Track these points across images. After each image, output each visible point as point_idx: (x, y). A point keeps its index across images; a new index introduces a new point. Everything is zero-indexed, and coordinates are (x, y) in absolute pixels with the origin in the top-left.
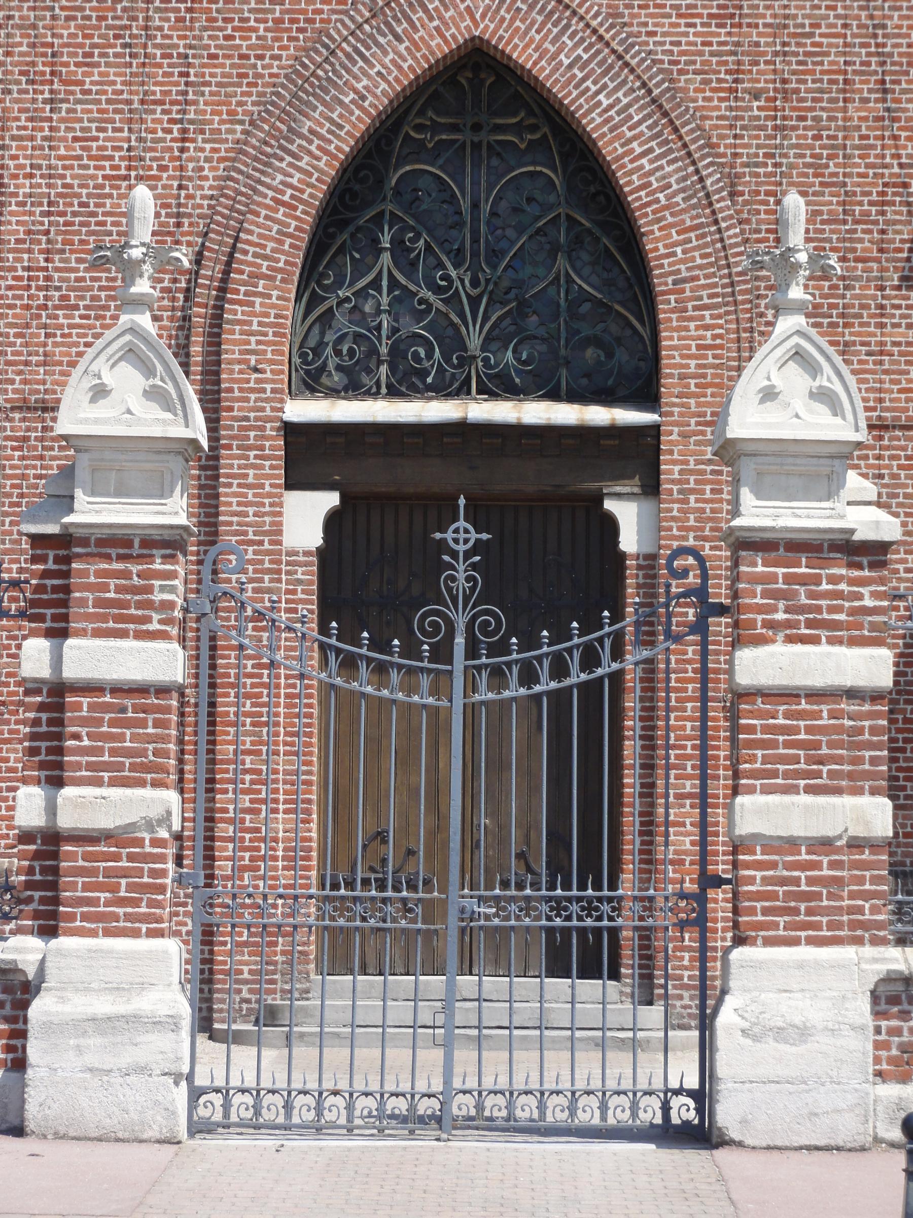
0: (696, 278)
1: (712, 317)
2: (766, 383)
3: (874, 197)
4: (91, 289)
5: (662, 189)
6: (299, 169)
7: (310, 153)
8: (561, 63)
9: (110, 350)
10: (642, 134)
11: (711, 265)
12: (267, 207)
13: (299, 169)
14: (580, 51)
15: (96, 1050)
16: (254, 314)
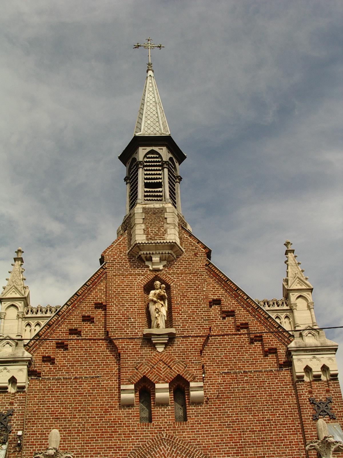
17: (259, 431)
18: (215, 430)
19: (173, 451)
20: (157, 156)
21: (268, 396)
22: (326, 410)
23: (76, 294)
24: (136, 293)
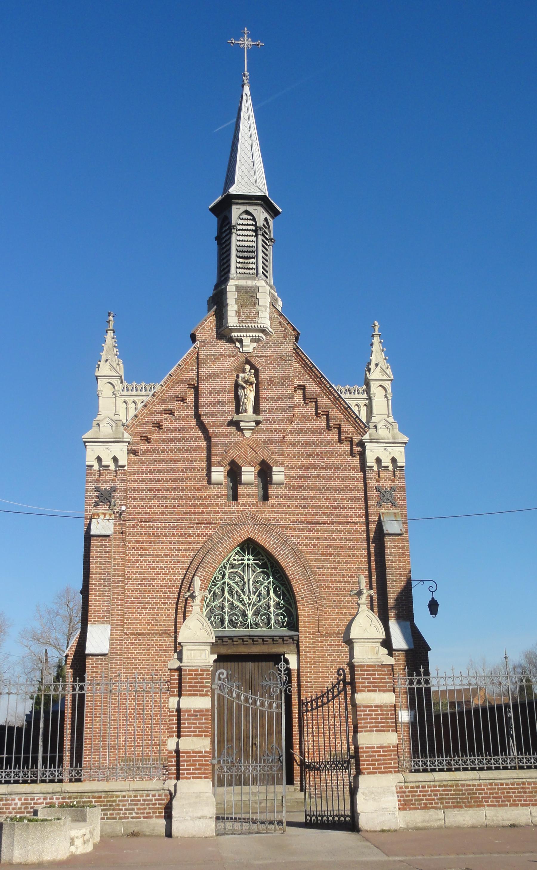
4: (151, 603)
5: (297, 575)
6: (206, 571)
11: (310, 594)
13: (206, 571)
18: (292, 511)
20: (252, 218)
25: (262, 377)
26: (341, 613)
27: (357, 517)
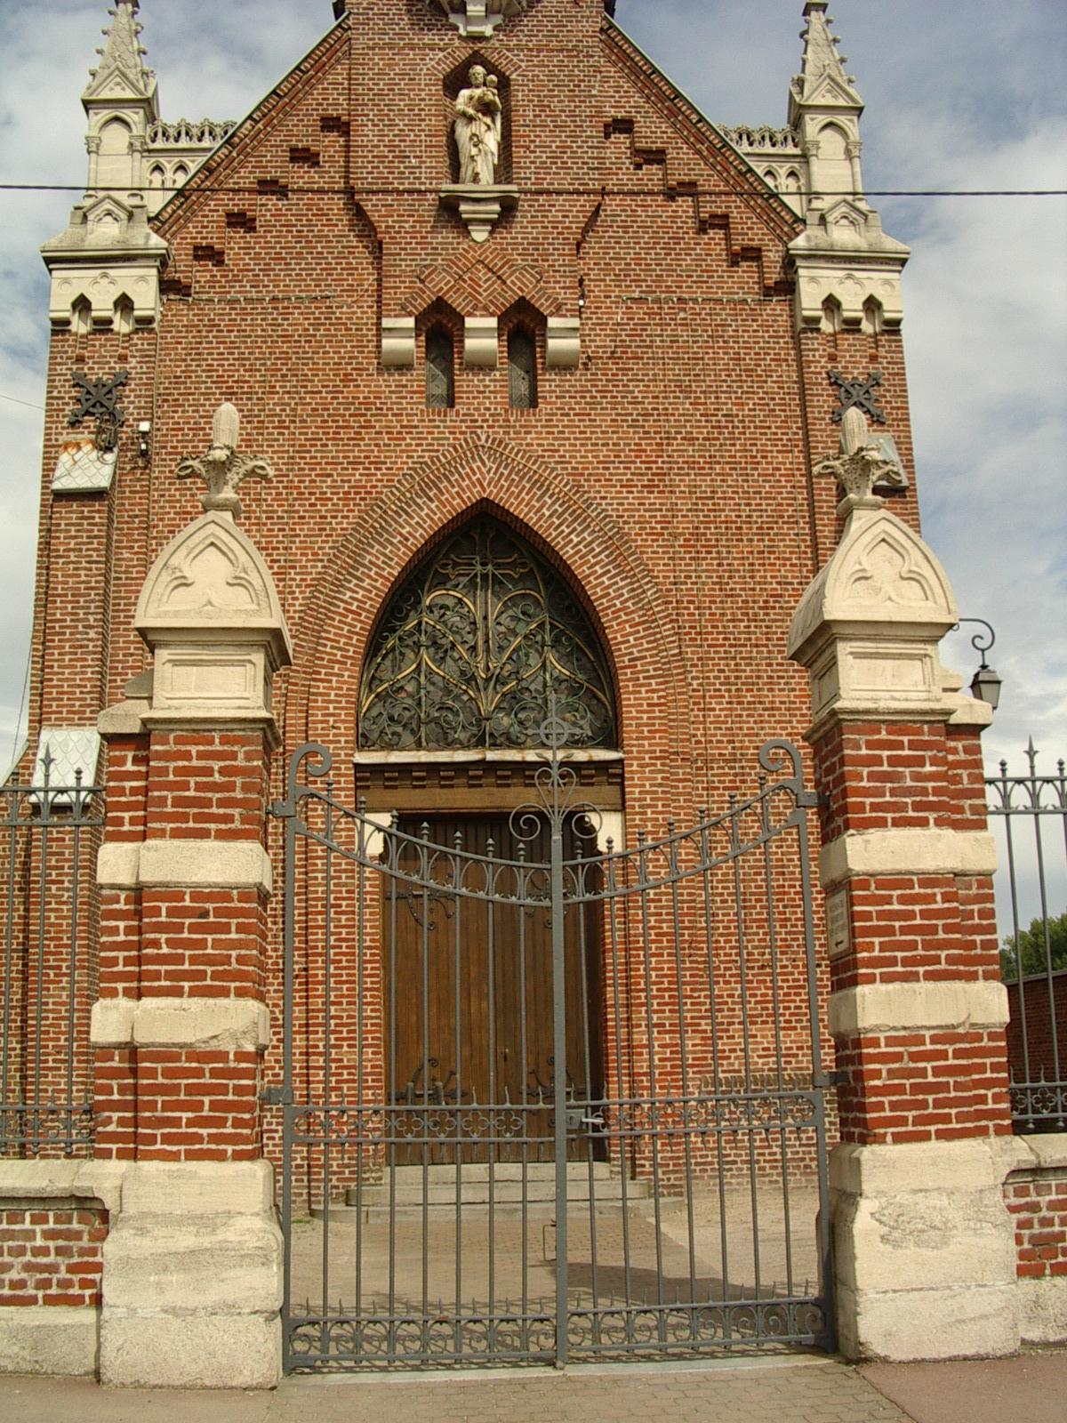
0: (645, 657)
1: (657, 684)
2: (858, 567)
3: (761, 604)
6: (363, 588)
7: (369, 577)
8: (543, 515)
9: (190, 543)
10: (602, 560)
11: (654, 648)
12: (341, 614)
13: (363, 588)
14: (556, 506)
15: (179, 1289)
16: (332, 688)
17: (704, 439)
18: (602, 432)
19: (502, 474)
21: (732, 359)
22: (864, 402)
23: (274, 92)
24: (423, 93)
25: (519, 96)
26: (739, 703)
27: (778, 451)
